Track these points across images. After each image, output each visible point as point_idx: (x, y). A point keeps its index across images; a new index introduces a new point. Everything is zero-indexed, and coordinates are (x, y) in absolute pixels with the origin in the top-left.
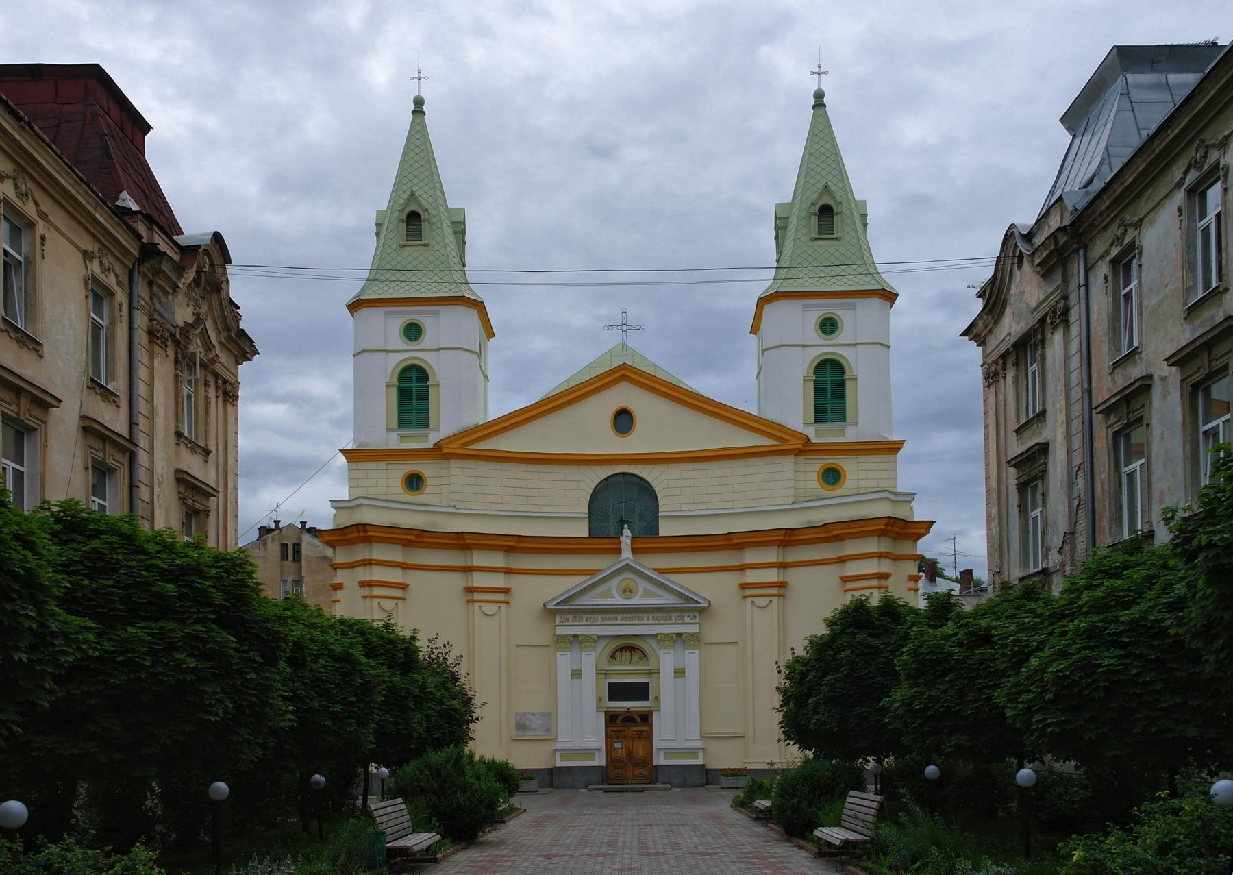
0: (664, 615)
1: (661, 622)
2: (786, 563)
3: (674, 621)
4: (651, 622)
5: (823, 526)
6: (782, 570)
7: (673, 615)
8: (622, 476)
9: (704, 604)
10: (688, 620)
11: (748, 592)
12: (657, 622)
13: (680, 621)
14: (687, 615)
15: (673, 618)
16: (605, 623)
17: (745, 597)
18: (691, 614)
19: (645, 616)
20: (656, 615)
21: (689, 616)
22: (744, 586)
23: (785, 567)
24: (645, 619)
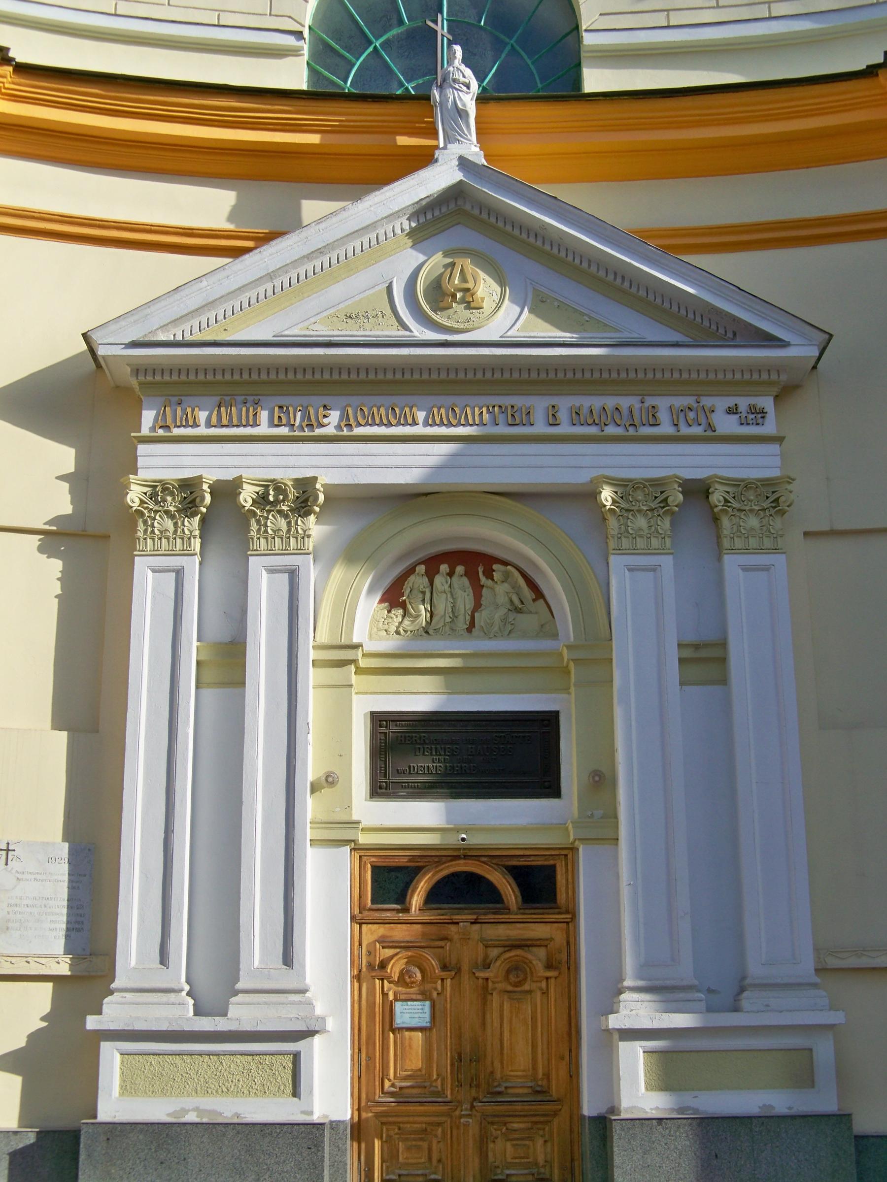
0: (625, 402)
1: (611, 430)
3: (666, 429)
4: (564, 429)
7: (663, 403)
10: (727, 424)
12: (593, 430)
13: (697, 430)
14: (721, 403)
15: (663, 416)
18: (743, 403)
19: (539, 405)
20: (586, 402)
21: (733, 410)
24: (539, 416)
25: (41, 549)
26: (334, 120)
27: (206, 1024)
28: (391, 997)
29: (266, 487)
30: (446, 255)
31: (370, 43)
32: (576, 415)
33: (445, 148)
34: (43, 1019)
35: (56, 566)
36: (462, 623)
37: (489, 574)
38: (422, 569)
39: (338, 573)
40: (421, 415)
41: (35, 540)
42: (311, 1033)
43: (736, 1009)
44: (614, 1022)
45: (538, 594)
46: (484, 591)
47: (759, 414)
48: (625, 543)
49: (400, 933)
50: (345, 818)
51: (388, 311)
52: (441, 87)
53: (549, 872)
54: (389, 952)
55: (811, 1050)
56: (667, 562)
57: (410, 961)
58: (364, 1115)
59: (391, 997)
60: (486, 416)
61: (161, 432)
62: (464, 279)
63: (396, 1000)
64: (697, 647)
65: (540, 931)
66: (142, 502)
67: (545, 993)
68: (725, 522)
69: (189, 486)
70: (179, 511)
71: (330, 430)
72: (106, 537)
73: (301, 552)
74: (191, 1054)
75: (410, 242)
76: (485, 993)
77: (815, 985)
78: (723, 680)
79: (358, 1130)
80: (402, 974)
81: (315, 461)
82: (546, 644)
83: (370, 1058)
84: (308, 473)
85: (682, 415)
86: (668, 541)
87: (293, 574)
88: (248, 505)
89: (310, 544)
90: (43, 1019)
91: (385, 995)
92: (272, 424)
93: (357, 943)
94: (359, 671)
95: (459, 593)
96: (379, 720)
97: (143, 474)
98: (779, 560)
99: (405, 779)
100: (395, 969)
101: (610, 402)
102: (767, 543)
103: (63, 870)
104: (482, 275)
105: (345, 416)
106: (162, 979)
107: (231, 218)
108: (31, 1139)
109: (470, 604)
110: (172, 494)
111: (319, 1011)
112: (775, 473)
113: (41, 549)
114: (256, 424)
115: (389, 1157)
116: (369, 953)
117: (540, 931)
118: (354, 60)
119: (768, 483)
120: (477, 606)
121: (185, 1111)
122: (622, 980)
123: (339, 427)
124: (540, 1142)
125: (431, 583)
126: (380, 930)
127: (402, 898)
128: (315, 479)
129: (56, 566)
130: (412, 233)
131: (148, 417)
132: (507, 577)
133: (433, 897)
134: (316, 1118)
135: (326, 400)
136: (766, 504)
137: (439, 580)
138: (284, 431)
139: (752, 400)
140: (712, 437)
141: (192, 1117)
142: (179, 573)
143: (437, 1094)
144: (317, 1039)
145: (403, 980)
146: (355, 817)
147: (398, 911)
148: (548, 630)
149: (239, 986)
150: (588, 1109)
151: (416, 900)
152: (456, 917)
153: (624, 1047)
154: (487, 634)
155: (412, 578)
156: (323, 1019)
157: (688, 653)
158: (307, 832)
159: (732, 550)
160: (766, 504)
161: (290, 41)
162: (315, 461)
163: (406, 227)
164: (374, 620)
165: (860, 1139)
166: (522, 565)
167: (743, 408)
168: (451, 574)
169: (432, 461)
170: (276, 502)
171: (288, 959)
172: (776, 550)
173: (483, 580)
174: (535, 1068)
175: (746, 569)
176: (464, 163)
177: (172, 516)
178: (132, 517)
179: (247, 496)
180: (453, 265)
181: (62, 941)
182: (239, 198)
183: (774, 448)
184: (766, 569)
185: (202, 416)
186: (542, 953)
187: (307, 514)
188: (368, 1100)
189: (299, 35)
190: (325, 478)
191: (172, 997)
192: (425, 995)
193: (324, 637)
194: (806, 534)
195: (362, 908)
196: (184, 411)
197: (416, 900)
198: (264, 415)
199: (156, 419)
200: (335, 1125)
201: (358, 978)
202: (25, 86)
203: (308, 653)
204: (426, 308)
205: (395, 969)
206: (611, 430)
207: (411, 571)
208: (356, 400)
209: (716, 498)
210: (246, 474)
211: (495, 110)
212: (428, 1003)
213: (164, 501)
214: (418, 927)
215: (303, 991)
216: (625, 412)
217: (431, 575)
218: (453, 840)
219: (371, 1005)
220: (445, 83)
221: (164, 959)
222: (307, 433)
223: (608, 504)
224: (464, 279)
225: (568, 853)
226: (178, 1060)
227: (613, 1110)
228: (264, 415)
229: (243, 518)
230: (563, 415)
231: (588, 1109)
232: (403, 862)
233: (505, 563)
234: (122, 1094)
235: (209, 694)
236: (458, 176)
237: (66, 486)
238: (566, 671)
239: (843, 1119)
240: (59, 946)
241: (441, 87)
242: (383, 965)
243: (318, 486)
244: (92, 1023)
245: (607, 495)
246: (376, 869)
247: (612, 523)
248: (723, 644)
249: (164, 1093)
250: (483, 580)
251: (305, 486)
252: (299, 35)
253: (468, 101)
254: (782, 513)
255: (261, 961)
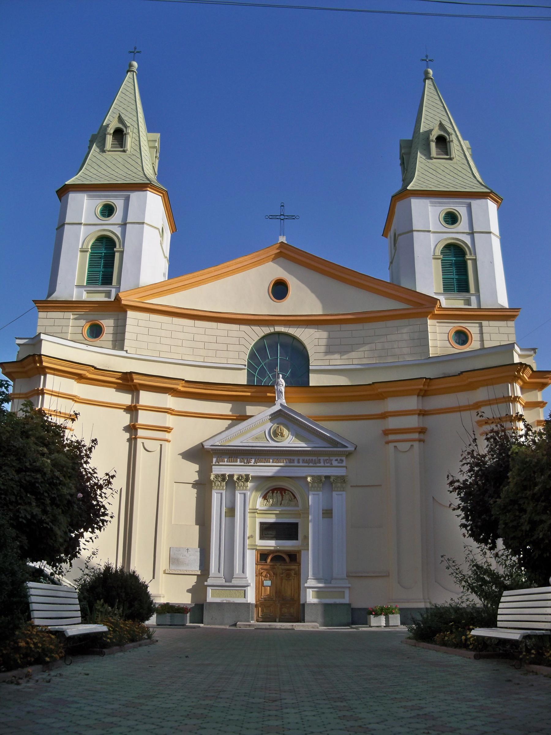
0: (314, 458)
2: (425, 411)
3: (322, 464)
4: (301, 464)
5: (459, 374)
6: (421, 417)
7: (322, 458)
8: (277, 336)
9: (351, 448)
10: (335, 463)
11: (391, 437)
12: (307, 464)
13: (329, 464)
14: (334, 458)
15: (322, 461)
16: (258, 464)
17: (388, 443)
18: (339, 458)
19: (296, 458)
21: (336, 460)
22: (386, 432)
23: (424, 415)
24: (296, 461)
25: (192, 487)
26: (253, 390)
27: (227, 584)
28: (263, 580)
29: (239, 476)
30: (277, 424)
31: (261, 364)
32: (304, 461)
33: (277, 401)
34: (195, 583)
35: (195, 490)
36: (279, 503)
37: (285, 493)
38: (271, 492)
39: (254, 493)
40: (271, 461)
41: (191, 485)
42: (248, 586)
43: (331, 583)
44: (306, 585)
45: (295, 497)
46: (284, 496)
47: (342, 461)
48: (312, 489)
49: (265, 567)
50: (254, 544)
51: (265, 437)
52: (277, 385)
53: (295, 556)
54: (263, 571)
55: (344, 591)
56: (321, 493)
57: (267, 573)
58: (257, 603)
59: (263, 580)
60: (285, 461)
61: (217, 463)
62: (281, 430)
63: (264, 580)
64: (326, 510)
65: (293, 567)
66: (214, 478)
67: (294, 579)
68: (334, 485)
69: (223, 476)
70: (221, 480)
71: (252, 464)
72: (206, 484)
73: (246, 490)
74: (224, 590)
75: (270, 421)
76: (282, 579)
77: (346, 579)
78: (331, 517)
79: (256, 606)
80: (265, 575)
81: (249, 470)
82: (296, 508)
83: (259, 592)
84: (248, 473)
85: (326, 461)
86: (321, 489)
87: (245, 494)
88: (235, 480)
89: (248, 488)
90: (195, 583)
91: (262, 579)
92: (240, 462)
93: (256, 569)
94: (258, 513)
95: (279, 498)
96: (262, 524)
97: (214, 473)
98: (344, 493)
99: (266, 536)
100: (264, 574)
101: (311, 458)
102: (342, 489)
103: (198, 554)
104: (285, 429)
105: (255, 461)
106: (219, 575)
107: (231, 411)
108: (194, 605)
109: (281, 500)
110: (220, 477)
111: (249, 582)
112: (344, 474)
113: (192, 487)
114: (237, 462)
115: (262, 611)
116: (259, 571)
117: (293, 567)
118: (277, 620)
119: (343, 476)
120: (282, 500)
121: (224, 600)
122: (308, 577)
123: (254, 463)
124: (292, 609)
125: (273, 495)
126: (261, 566)
127: (266, 560)
128: (249, 475)
129: (195, 490)
130: (270, 419)
131: (214, 460)
132: (288, 494)
133: (271, 560)
134: (249, 602)
135: (251, 457)
136: (342, 481)
137: (274, 494)
138: (243, 464)
139: (340, 458)
140: (332, 466)
141: (225, 602)
142: (221, 494)
143: (272, 599)
144: (249, 587)
145: (266, 576)
146: (256, 544)
147: (265, 563)
148: (297, 505)
149: (234, 577)
150: (301, 602)
151: (269, 560)
152: (277, 564)
153: (308, 590)
154: (284, 506)
155: (269, 494)
156: (250, 583)
157: (324, 512)
158: (247, 547)
159: (334, 491)
160: (342, 481)
161: (243, 367)
162: (249, 470)
163: (269, 418)
164: (261, 503)
165: (352, 609)
166: (292, 491)
167: (339, 459)
168: (277, 493)
169: (274, 471)
170: (241, 479)
171: (243, 572)
172: (343, 491)
173: (283, 494)
174: (291, 594)
175: (337, 494)
176: (281, 405)
177: (220, 482)
178: (211, 482)
179: (235, 478)
180: (278, 427)
181: (199, 568)
182: (232, 406)
183: (345, 469)
184: (341, 495)
185: (226, 460)
186: (293, 572)
187: (248, 482)
188: (258, 600)
189: (245, 365)
190: (251, 474)
191: (221, 579)
192: (270, 580)
193: (251, 507)
194: (351, 486)
195: (258, 562)
196: (222, 459)
197: (269, 560)
198: (239, 460)
199: (216, 461)
200: (252, 604)
201: (256, 576)
202: (187, 385)
203: (248, 510)
204: (273, 437)
205: (264, 574)
206: (311, 464)
207: (268, 492)
208: (258, 457)
209: (332, 480)
210: (235, 473)
211: (288, 389)
212: (270, 581)
213: (218, 478)
214: (269, 566)
215: (246, 578)
216: (314, 461)
217: (273, 493)
218: (276, 549)
219: (259, 581)
220: (278, 384)
221: (219, 572)
222: (247, 464)
223: (309, 481)
224: (281, 430)
225: (299, 552)
226: (222, 591)
227: (306, 602)
228: (239, 460)
229: (234, 482)
230: (301, 461)
231: (301, 602)
232: (266, 553)
233: (288, 491)
234: (211, 597)
235: (227, 518)
236: (280, 408)
237: (197, 473)
238: (300, 514)
239: (349, 605)
240: (198, 568)
241: (277, 385)
242: (262, 573)
243: (250, 476)
244: (206, 583)
245: (309, 479)
246: (260, 554)
247: (310, 485)
248: (332, 510)
249: (219, 597)
250: (283, 494)
251: (247, 476)
252: (245, 365)
253: (283, 389)
254: (345, 483)
255: (238, 572)
